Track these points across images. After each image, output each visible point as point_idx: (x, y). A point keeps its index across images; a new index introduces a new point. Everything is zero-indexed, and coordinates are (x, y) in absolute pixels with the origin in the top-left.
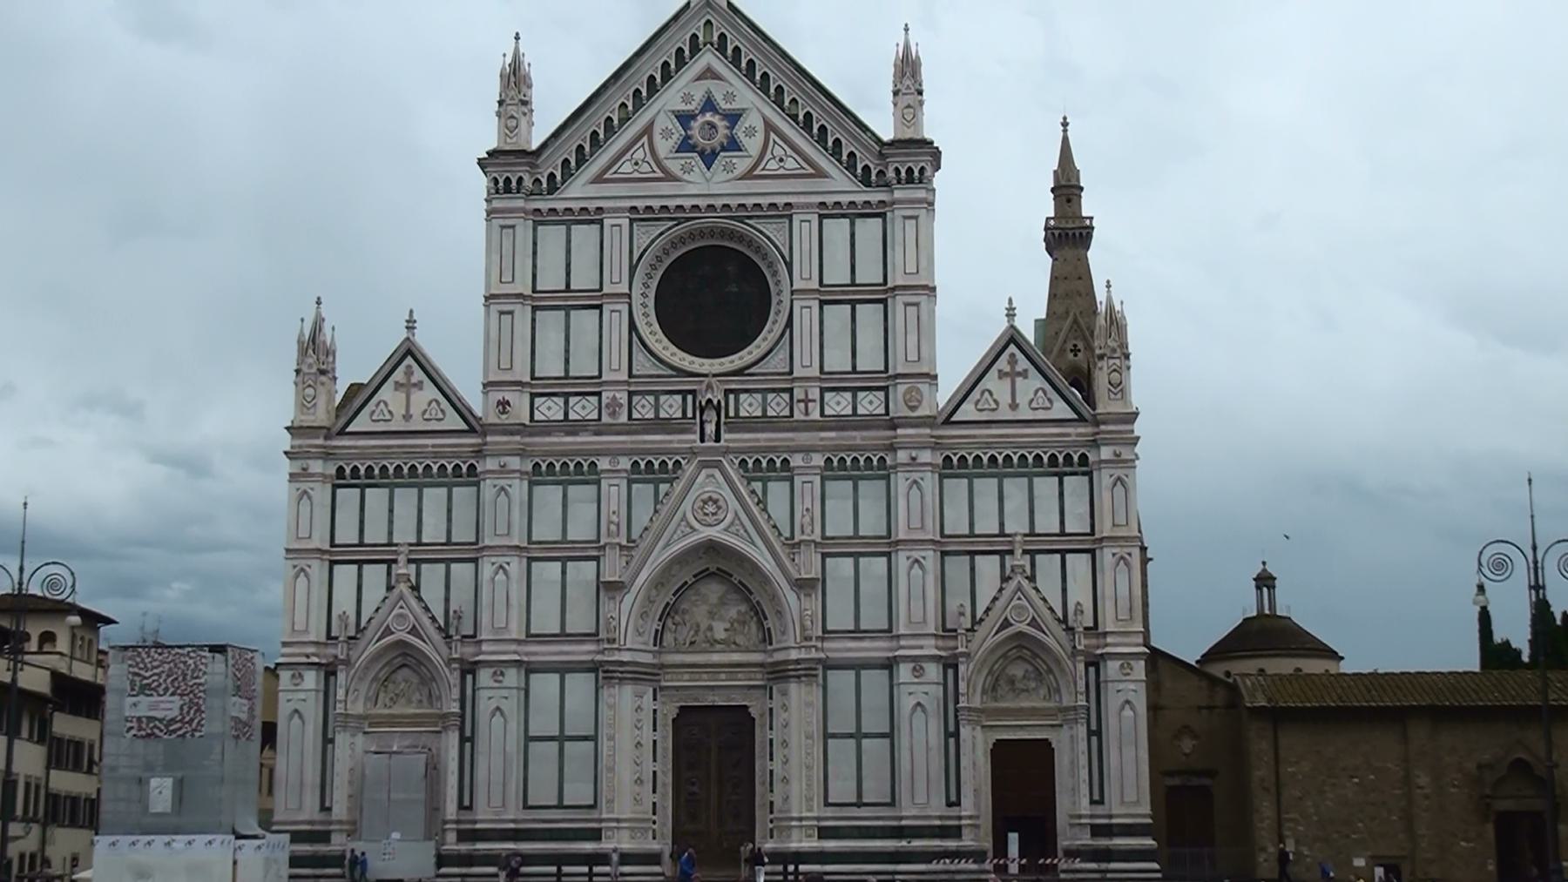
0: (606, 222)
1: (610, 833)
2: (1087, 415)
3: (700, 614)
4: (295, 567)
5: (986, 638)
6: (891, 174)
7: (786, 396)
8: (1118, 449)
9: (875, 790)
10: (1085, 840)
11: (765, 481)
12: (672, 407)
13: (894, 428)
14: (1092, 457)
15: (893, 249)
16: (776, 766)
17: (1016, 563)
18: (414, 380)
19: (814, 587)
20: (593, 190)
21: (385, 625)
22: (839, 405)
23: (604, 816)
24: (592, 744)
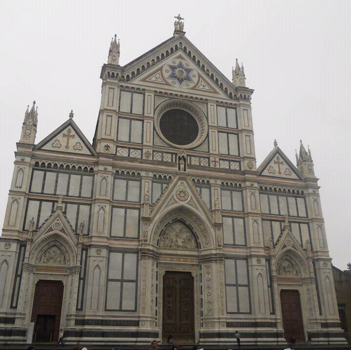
0: (146, 94)
1: (144, 323)
2: (302, 178)
3: (172, 235)
4: (13, 198)
5: (278, 252)
6: (238, 95)
7: (207, 160)
8: (315, 190)
9: (244, 307)
10: (318, 329)
11: (201, 187)
12: (168, 158)
13: (244, 175)
14: (305, 192)
15: (240, 118)
16: (205, 297)
17: (286, 224)
18: (71, 134)
19: (220, 227)
20: (142, 83)
21: (50, 227)
22: (225, 165)
23: (141, 315)
24: (134, 284)
